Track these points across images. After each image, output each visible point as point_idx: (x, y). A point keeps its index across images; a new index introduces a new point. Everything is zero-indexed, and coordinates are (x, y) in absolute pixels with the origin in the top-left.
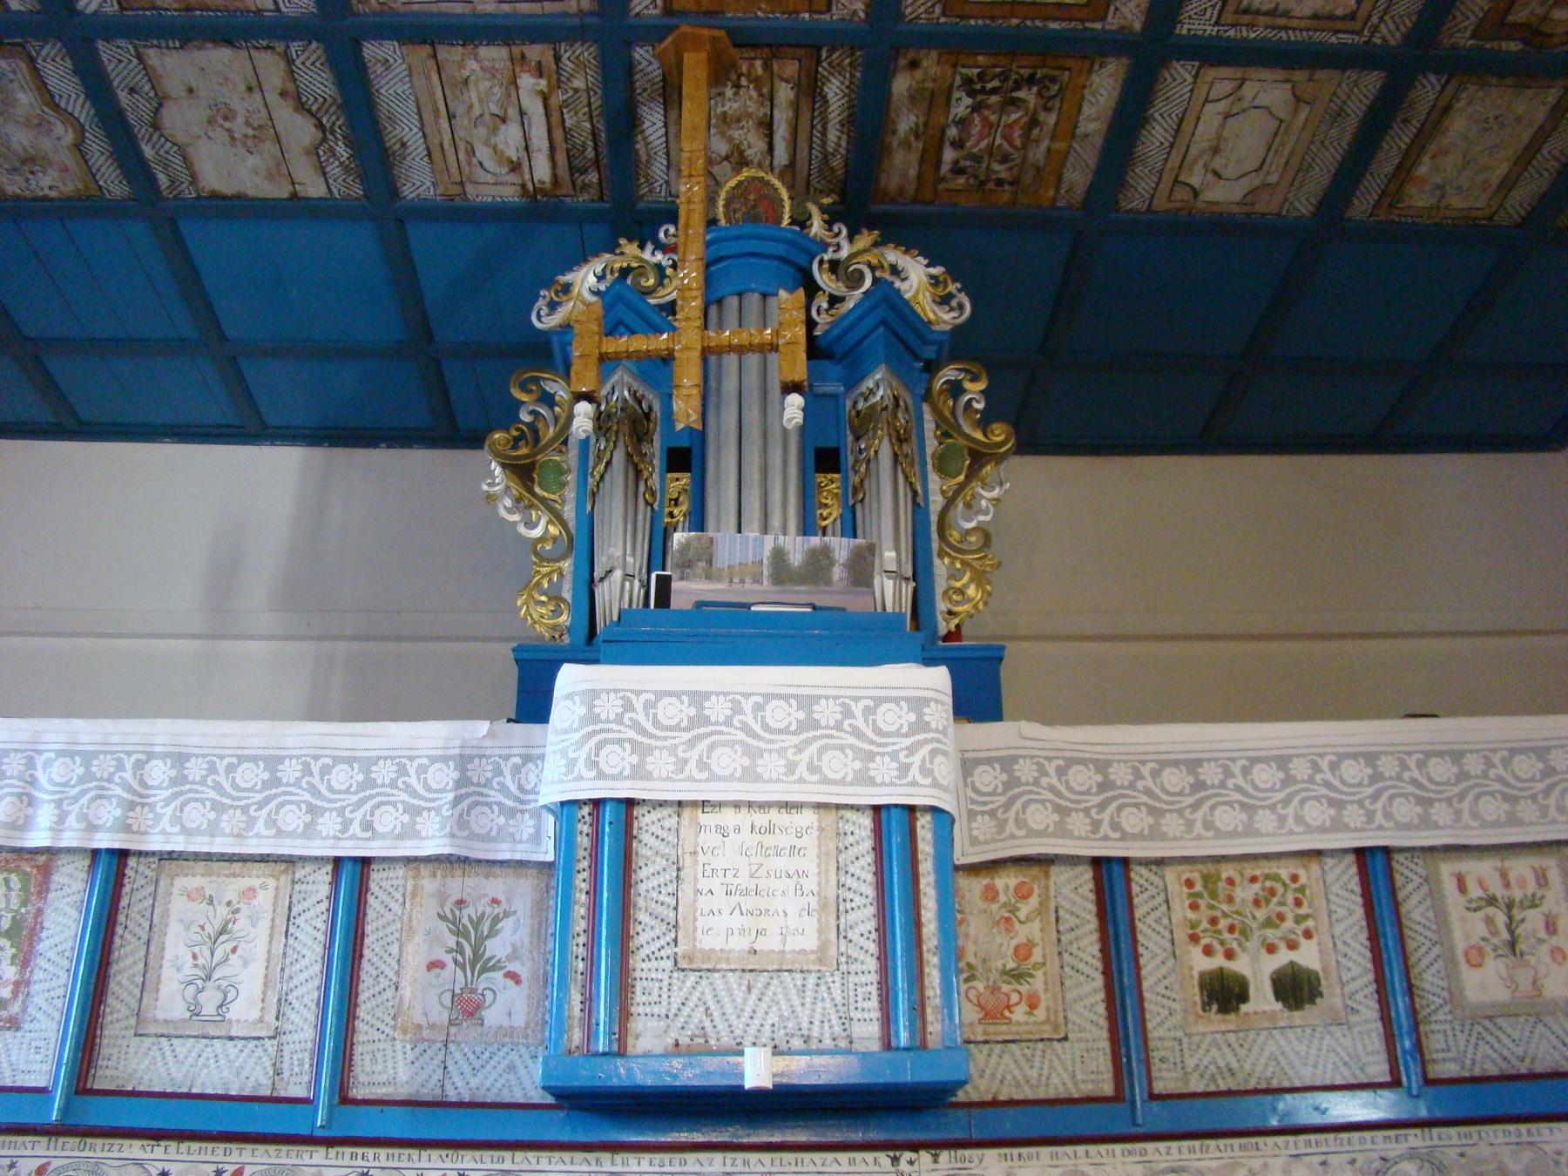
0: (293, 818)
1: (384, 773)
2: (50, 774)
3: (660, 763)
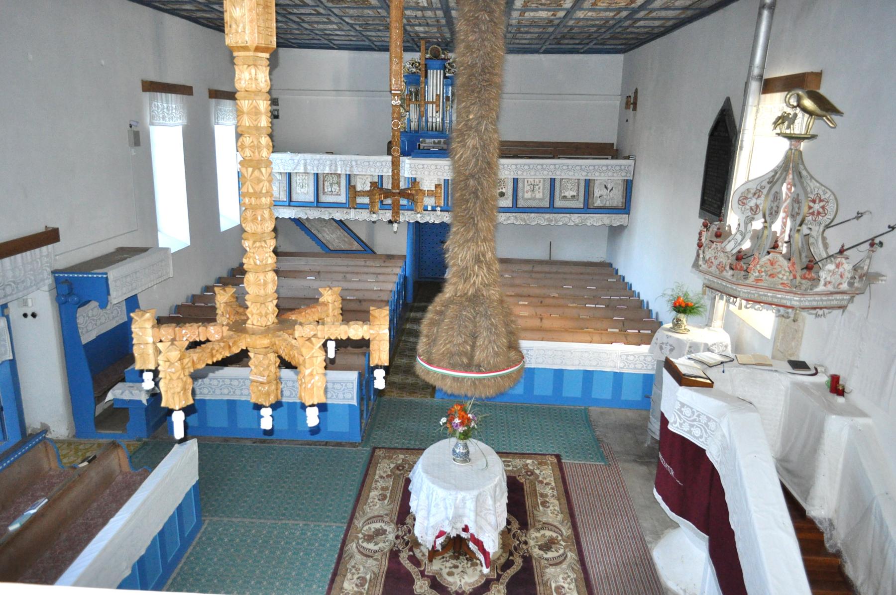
0: (373, 170)
1: (384, 164)
2: (339, 163)
3: (419, 173)
